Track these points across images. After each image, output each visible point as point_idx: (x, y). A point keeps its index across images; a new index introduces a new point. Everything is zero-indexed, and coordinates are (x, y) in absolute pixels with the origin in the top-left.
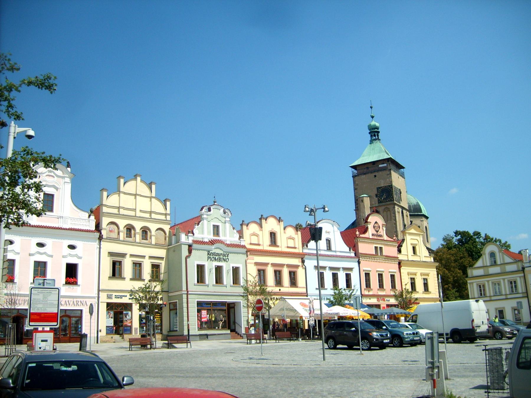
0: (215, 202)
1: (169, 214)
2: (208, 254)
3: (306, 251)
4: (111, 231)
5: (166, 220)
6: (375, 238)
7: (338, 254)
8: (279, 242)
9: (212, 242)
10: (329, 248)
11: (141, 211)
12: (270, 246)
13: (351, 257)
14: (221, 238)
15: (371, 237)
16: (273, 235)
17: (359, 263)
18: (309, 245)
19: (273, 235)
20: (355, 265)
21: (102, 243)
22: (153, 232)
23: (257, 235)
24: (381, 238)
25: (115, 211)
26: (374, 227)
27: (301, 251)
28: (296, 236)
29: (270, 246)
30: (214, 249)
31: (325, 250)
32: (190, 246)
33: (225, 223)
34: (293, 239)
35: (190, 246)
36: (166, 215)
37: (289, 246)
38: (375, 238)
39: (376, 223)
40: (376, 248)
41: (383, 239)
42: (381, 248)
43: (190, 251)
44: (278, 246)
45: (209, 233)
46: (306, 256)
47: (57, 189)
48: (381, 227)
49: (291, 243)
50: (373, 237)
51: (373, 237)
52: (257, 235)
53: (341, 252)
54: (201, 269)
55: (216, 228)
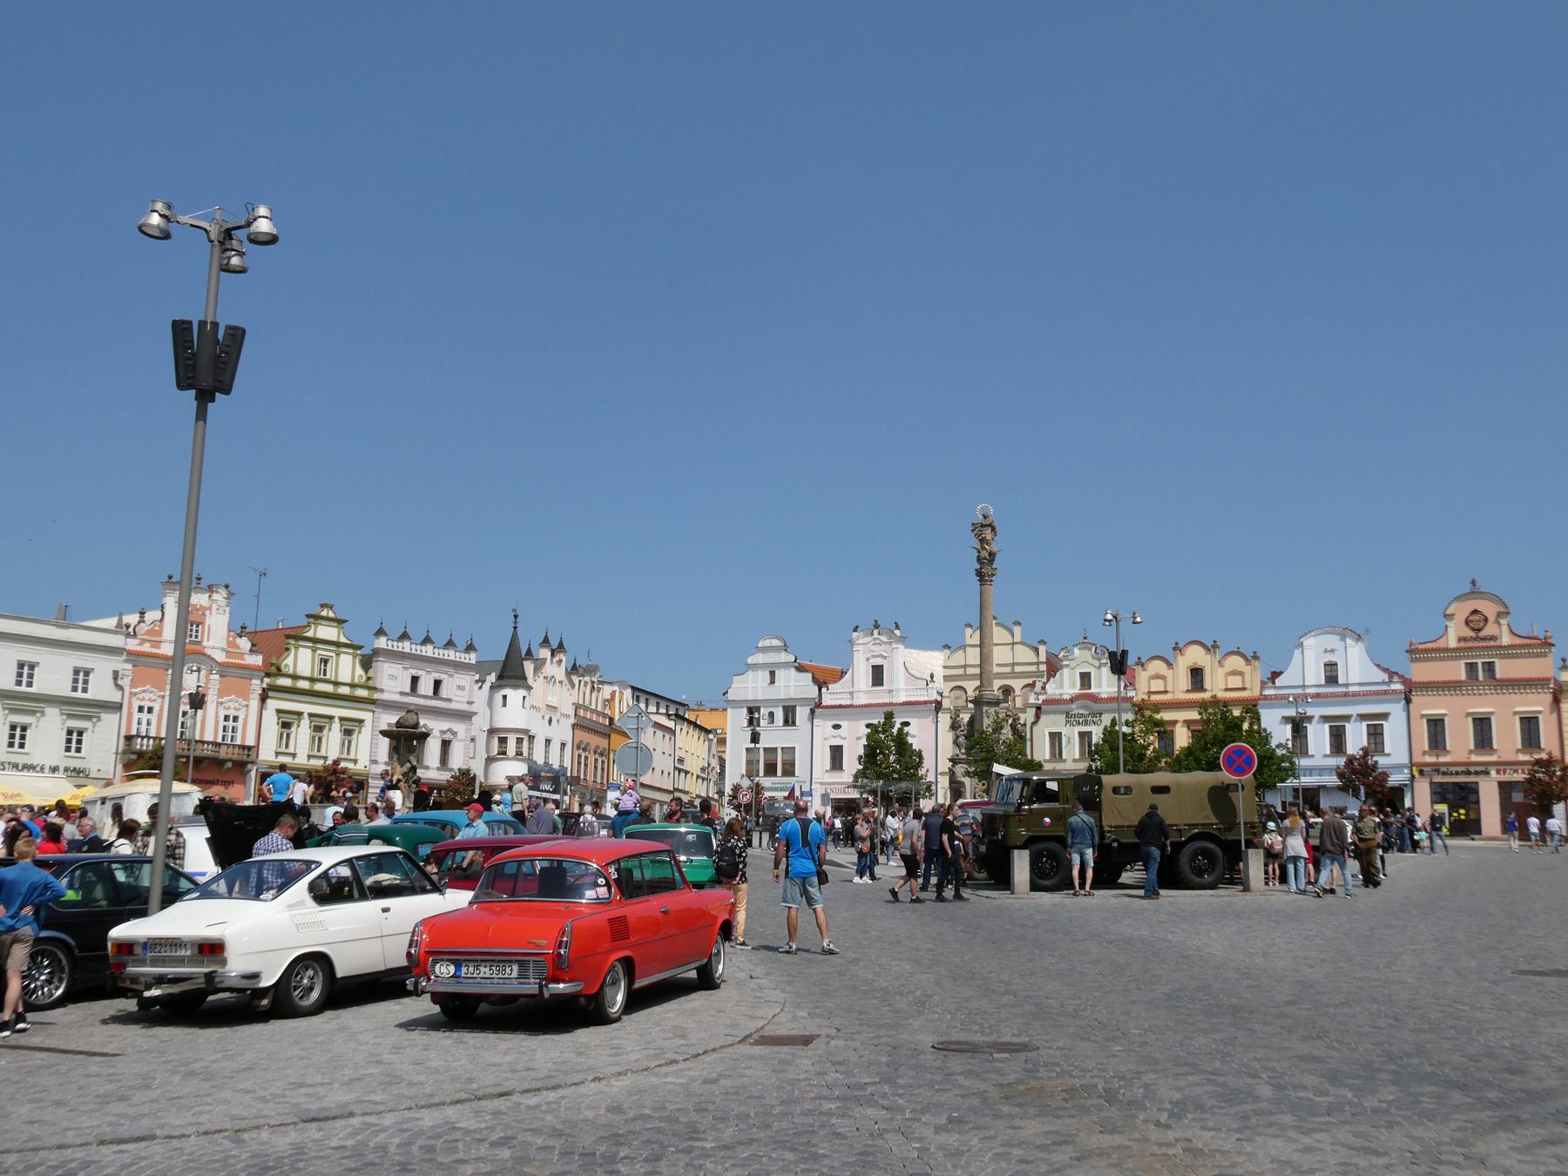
0: (1085, 638)
1: (1042, 663)
2: (1067, 716)
3: (1267, 692)
4: (957, 698)
5: (1039, 672)
6: (1470, 644)
7: (1352, 689)
8: (1207, 685)
9: (1072, 700)
10: (1332, 679)
11: (998, 665)
12: (1188, 691)
13: (1394, 691)
14: (1094, 690)
15: (1453, 643)
16: (1197, 674)
17: (1408, 701)
18: (1276, 680)
19: (1197, 674)
20: (1396, 710)
21: (940, 715)
22: (1018, 692)
23: (1163, 678)
24: (1492, 643)
25: (961, 672)
26: (1467, 623)
27: (1256, 693)
28: (1247, 669)
29: (1188, 691)
30: (1075, 709)
31: (1316, 686)
32: (1039, 708)
33: (1099, 667)
34: (1241, 674)
35: (1039, 708)
36: (1038, 664)
37: (1229, 686)
38: (1470, 644)
39: (1475, 612)
40: (1471, 668)
41: (1497, 643)
42: (1490, 667)
43: (1038, 717)
44: (1206, 690)
45: (1073, 686)
46: (1260, 702)
47: (885, 658)
48: (1491, 618)
49: (1235, 682)
50: (1462, 644)
51: (1462, 644)
52: (1163, 678)
53: (1360, 684)
54: (1056, 738)
55: (1085, 679)
